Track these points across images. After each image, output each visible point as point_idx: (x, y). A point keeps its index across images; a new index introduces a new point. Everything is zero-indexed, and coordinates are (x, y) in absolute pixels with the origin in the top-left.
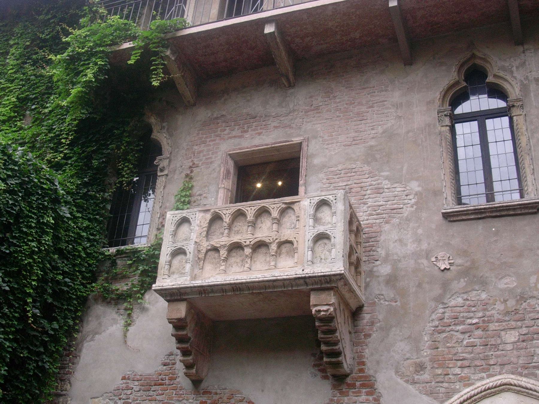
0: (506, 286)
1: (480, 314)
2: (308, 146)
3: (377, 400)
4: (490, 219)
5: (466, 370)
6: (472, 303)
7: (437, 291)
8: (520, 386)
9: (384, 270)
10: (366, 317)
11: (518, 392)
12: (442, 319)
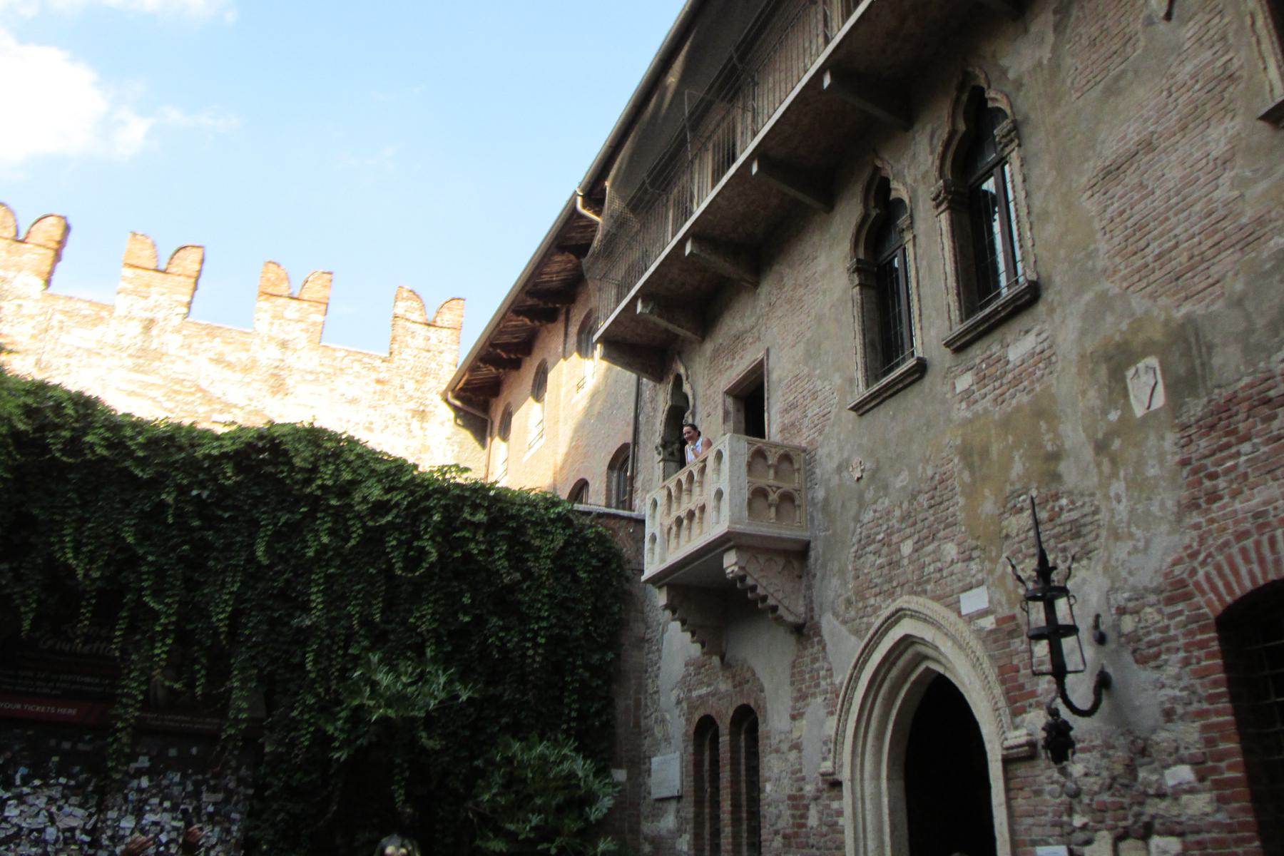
0: (901, 484)
1: (885, 527)
2: (768, 359)
3: (824, 648)
4: (888, 401)
5: (878, 598)
6: (878, 515)
7: (853, 507)
8: (909, 610)
9: (820, 494)
10: (812, 553)
11: (912, 616)
12: (860, 541)
